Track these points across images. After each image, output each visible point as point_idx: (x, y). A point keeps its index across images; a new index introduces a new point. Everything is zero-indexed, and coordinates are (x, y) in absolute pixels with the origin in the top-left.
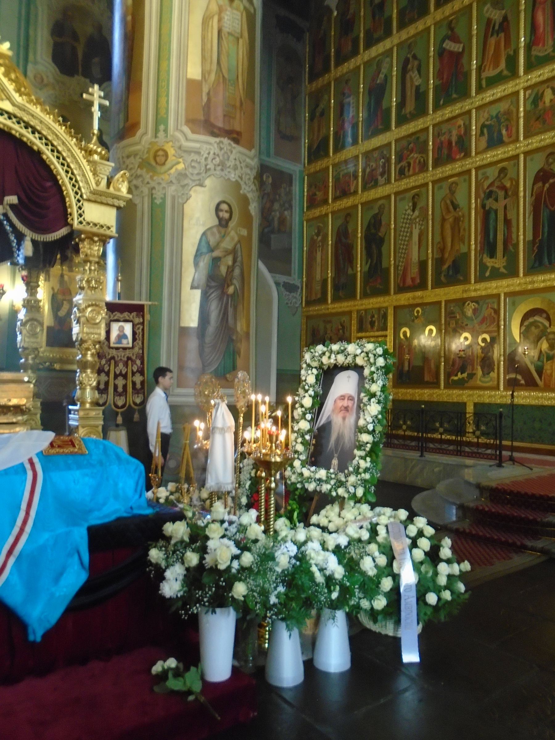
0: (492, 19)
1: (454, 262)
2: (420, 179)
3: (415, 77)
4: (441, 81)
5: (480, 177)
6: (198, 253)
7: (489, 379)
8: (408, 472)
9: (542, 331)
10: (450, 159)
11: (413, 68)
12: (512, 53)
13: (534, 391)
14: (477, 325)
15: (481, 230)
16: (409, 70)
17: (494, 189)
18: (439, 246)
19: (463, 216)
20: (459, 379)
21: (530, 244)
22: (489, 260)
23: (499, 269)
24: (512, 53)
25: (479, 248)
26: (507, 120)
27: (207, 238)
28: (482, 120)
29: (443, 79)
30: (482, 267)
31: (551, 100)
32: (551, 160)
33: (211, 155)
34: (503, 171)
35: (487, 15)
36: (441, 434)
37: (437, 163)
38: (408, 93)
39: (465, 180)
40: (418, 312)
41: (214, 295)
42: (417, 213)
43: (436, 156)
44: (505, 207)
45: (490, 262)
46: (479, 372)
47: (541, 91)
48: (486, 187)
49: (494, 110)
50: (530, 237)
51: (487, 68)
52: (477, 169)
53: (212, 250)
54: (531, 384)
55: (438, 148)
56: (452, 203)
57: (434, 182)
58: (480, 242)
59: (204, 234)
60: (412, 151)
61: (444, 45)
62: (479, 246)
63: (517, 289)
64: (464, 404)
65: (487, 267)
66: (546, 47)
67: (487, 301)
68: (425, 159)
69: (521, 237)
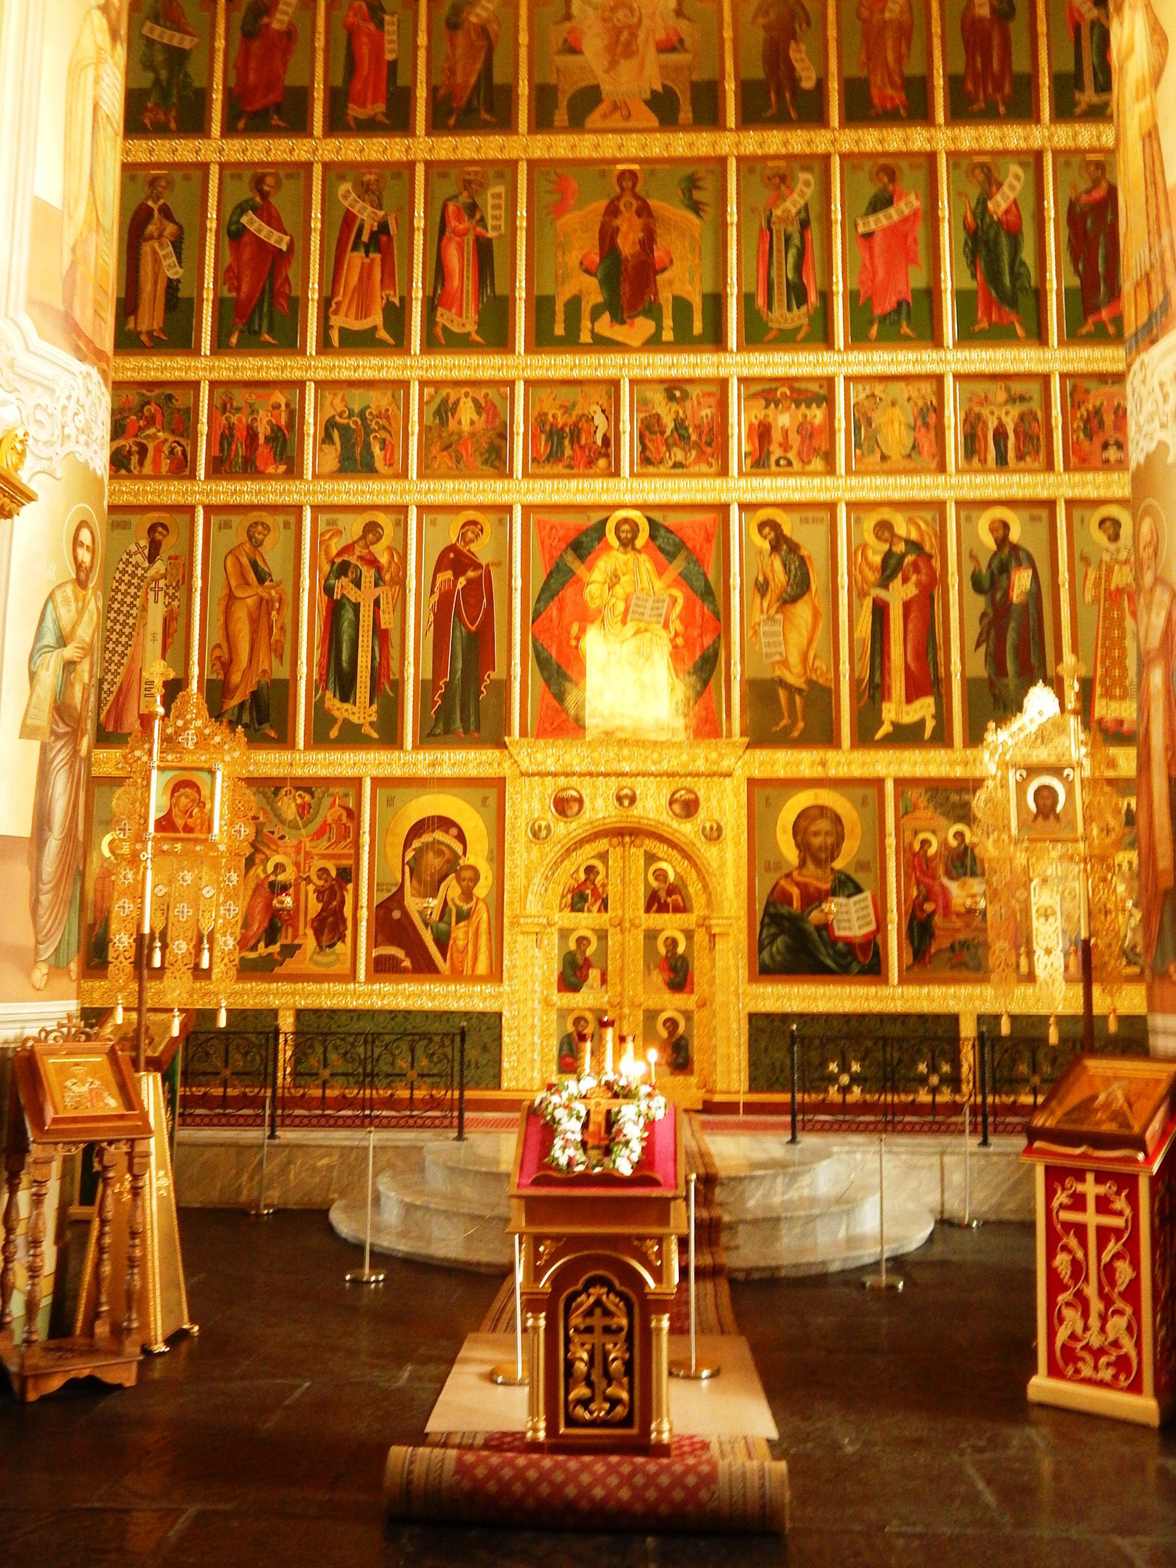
0: (355, 216)
1: (254, 694)
2: (172, 492)
3: (166, 257)
4: (234, 295)
6: (39, 645)
7: (333, 958)
8: (245, 1177)
9: (448, 862)
10: (250, 469)
11: (160, 236)
12: (397, 301)
13: (431, 981)
15: (323, 640)
16: (151, 237)
17: (353, 560)
18: (217, 653)
19: (280, 600)
20: (260, 956)
21: (426, 690)
22: (337, 703)
23: (361, 726)
24: (397, 301)
25: (315, 676)
26: (384, 428)
27: (55, 608)
28: (330, 412)
29: (238, 289)
31: (472, 423)
32: (470, 535)
33: (73, 407)
34: (372, 528)
35: (346, 204)
36: (225, 1085)
37: (219, 468)
38: (147, 288)
39: (286, 525)
41: (60, 758)
42: (160, 566)
43: (216, 452)
44: (377, 603)
46: (309, 942)
47: (452, 399)
48: (334, 552)
49: (357, 399)
51: (343, 309)
53: (63, 641)
54: (424, 967)
55: (223, 438)
56: (254, 565)
57: (209, 509)
58: (320, 665)
59: (51, 597)
60: (151, 421)
61: (244, 220)
62: (315, 669)
65: (335, 720)
66: (464, 320)
67: (332, 790)
68: (188, 449)
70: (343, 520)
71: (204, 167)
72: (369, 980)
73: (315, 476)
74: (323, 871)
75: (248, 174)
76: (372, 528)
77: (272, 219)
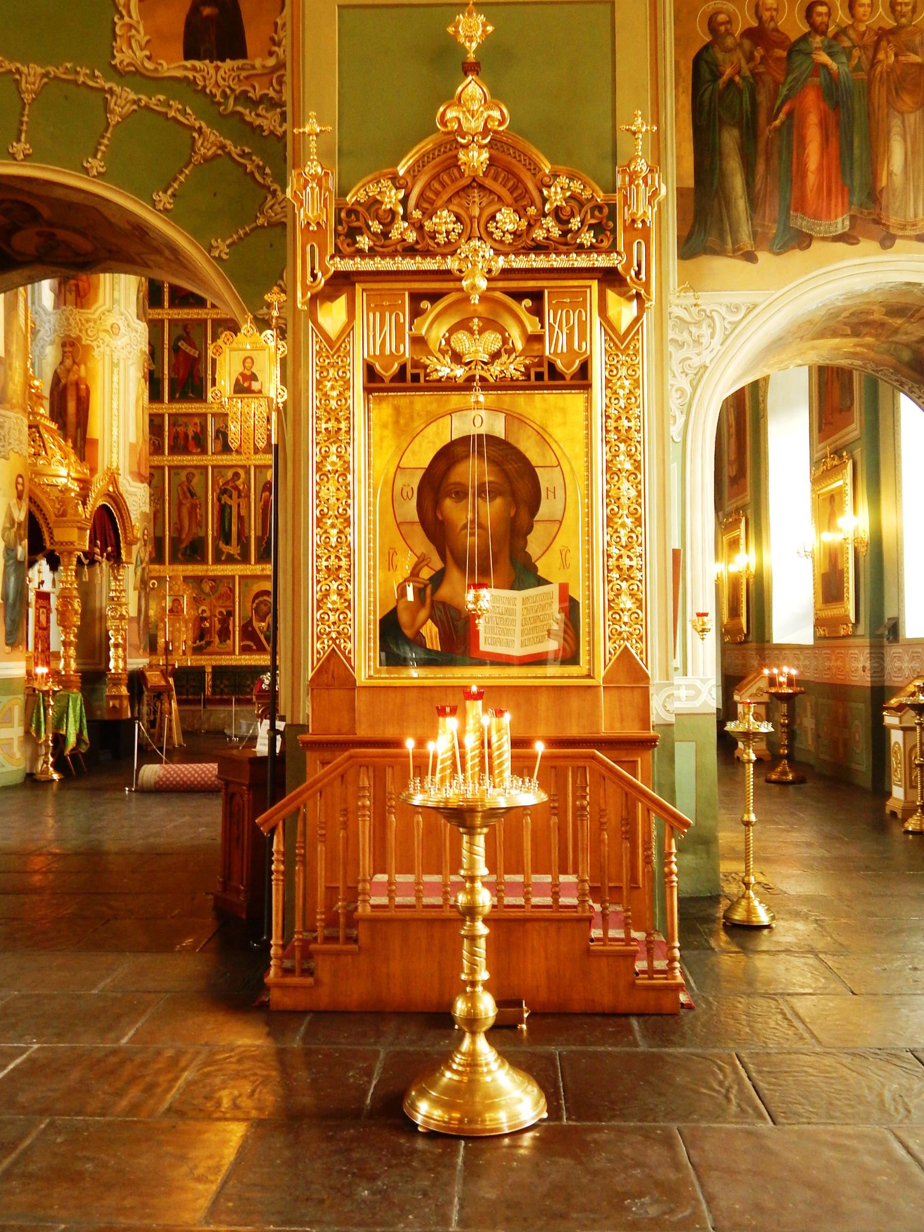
5: (215, 474)
10: (186, 451)
14: (214, 601)
17: (229, 488)
19: (200, 504)
23: (233, 555)
28: (218, 426)
30: (218, 553)
34: (236, 475)
37: (173, 451)
39: (202, 474)
40: (153, 584)
44: (239, 505)
45: (225, 548)
46: (217, 640)
50: (260, 533)
52: (213, 467)
53: (142, 563)
55: (174, 437)
56: (189, 490)
57: (170, 468)
63: (249, 573)
64: (203, 667)
65: (223, 552)
69: (253, 532)
70: (224, 471)
71: (162, 321)
72: (240, 654)
73: (213, 454)
74: (221, 613)
75: (180, 324)
76: (236, 475)
77: (192, 344)
